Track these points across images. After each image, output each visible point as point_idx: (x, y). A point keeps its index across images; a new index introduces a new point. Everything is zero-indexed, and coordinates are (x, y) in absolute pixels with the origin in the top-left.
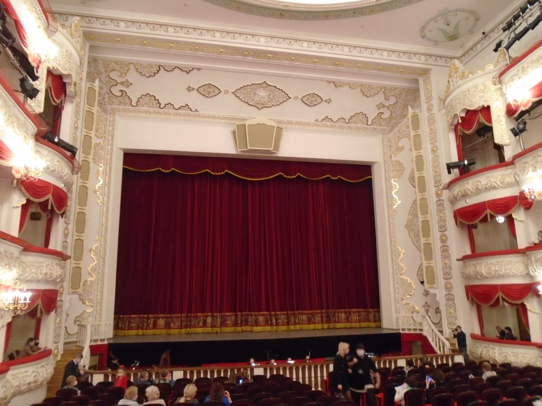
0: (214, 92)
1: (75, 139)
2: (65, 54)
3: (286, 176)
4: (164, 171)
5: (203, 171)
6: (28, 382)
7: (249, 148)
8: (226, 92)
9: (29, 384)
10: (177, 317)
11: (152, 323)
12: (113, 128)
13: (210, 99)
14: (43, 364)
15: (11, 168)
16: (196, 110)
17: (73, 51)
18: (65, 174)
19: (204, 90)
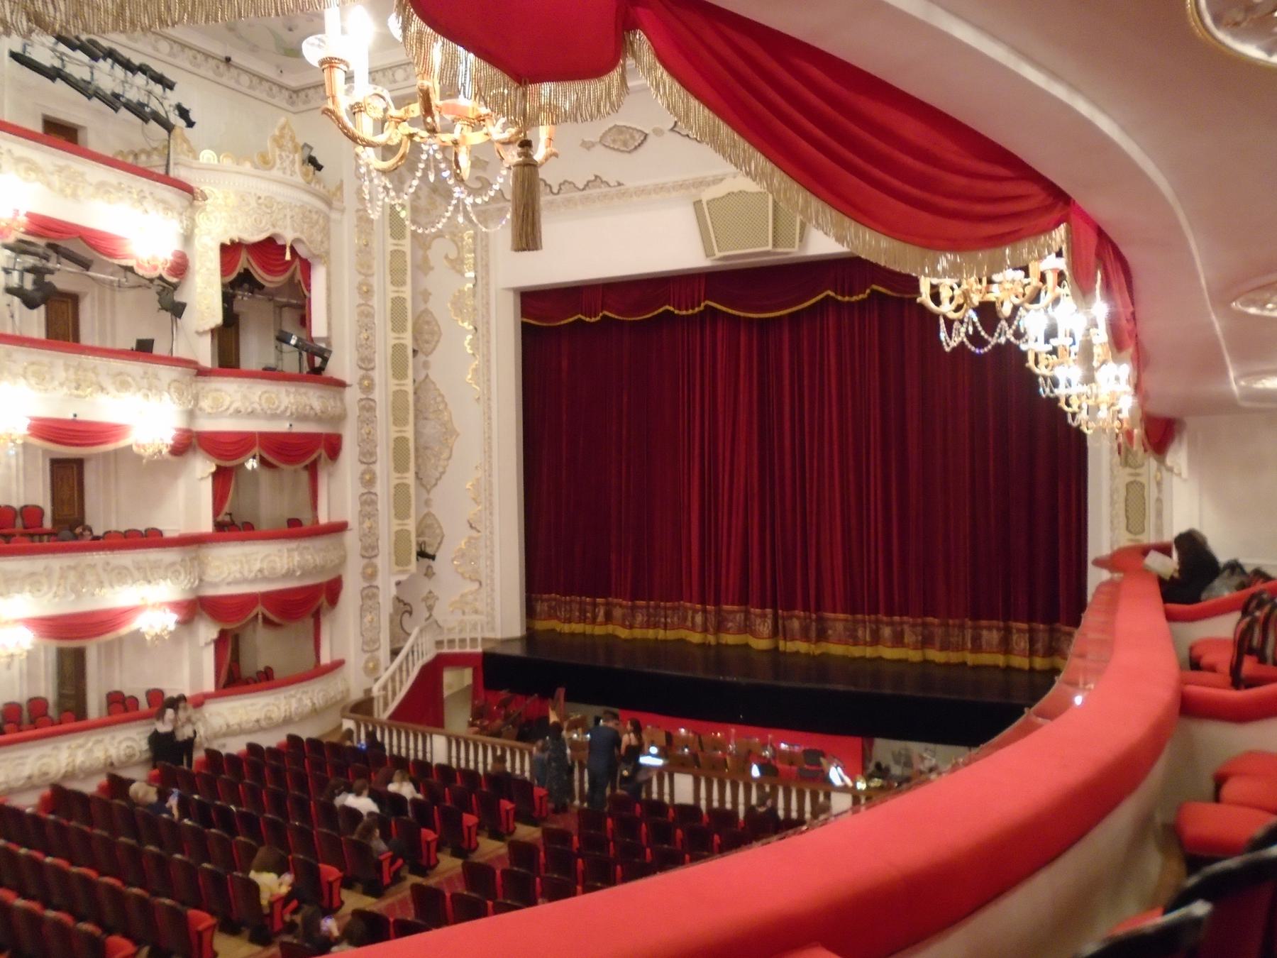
0: (633, 137)
1: (366, 316)
2: (253, 204)
3: (840, 298)
4: (588, 319)
5: (661, 310)
6: (254, 718)
7: (719, 254)
8: (658, 132)
9: (258, 721)
10: (641, 607)
11: (602, 613)
12: (487, 251)
13: (635, 154)
14: (293, 692)
15: (130, 447)
16: (619, 184)
17: (275, 188)
18: (282, 408)
19: (614, 141)
